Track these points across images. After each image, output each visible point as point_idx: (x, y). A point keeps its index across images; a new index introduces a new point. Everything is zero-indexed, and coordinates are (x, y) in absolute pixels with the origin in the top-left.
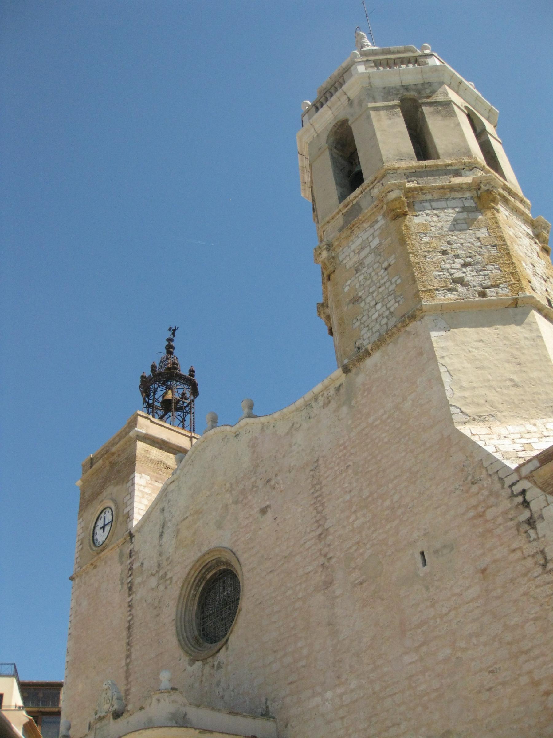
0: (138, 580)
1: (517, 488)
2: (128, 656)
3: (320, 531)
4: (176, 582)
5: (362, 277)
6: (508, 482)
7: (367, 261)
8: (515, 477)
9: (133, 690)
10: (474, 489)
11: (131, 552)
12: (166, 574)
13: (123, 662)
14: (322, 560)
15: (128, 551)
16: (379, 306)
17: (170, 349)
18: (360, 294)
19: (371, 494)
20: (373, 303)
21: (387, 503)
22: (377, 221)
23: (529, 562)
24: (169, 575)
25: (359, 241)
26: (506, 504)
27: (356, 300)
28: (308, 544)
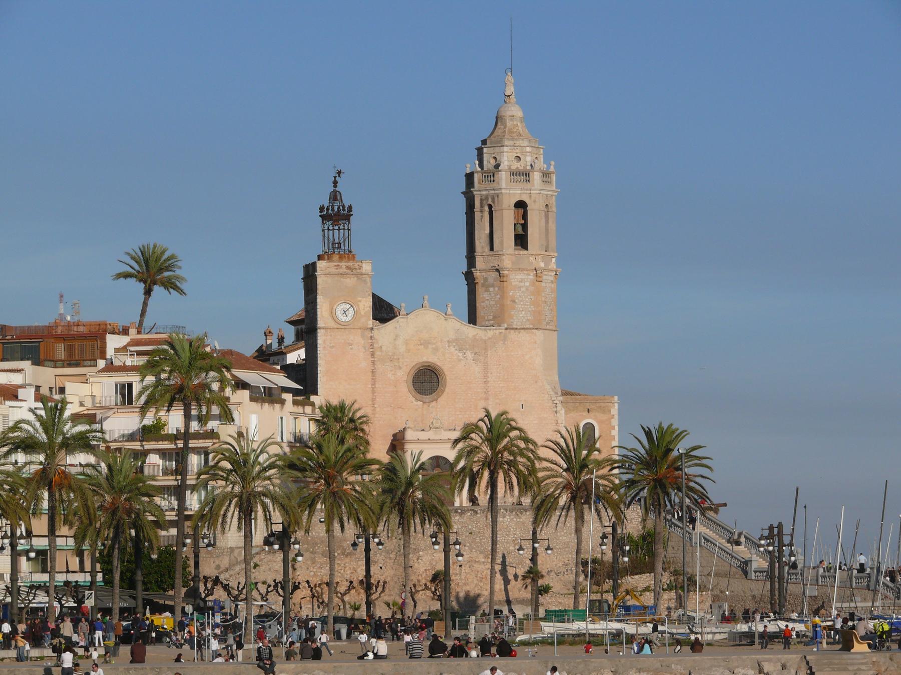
0: (378, 353)
1: (555, 402)
2: (372, 385)
3: (485, 380)
4: (407, 365)
5: (518, 294)
6: (553, 399)
7: (523, 289)
8: (555, 399)
9: (378, 399)
10: (543, 395)
11: (371, 337)
12: (399, 359)
13: (370, 386)
14: (485, 390)
15: (369, 335)
16: (523, 313)
17: (335, 183)
18: (516, 301)
19: (507, 378)
20: (521, 309)
21: (513, 384)
22: (530, 275)
23: (553, 421)
24: (401, 360)
25: (520, 277)
26: (550, 404)
27: (514, 301)
28: (479, 382)
